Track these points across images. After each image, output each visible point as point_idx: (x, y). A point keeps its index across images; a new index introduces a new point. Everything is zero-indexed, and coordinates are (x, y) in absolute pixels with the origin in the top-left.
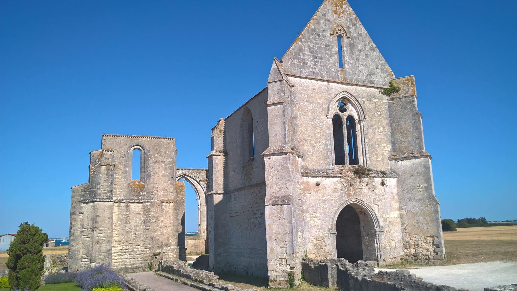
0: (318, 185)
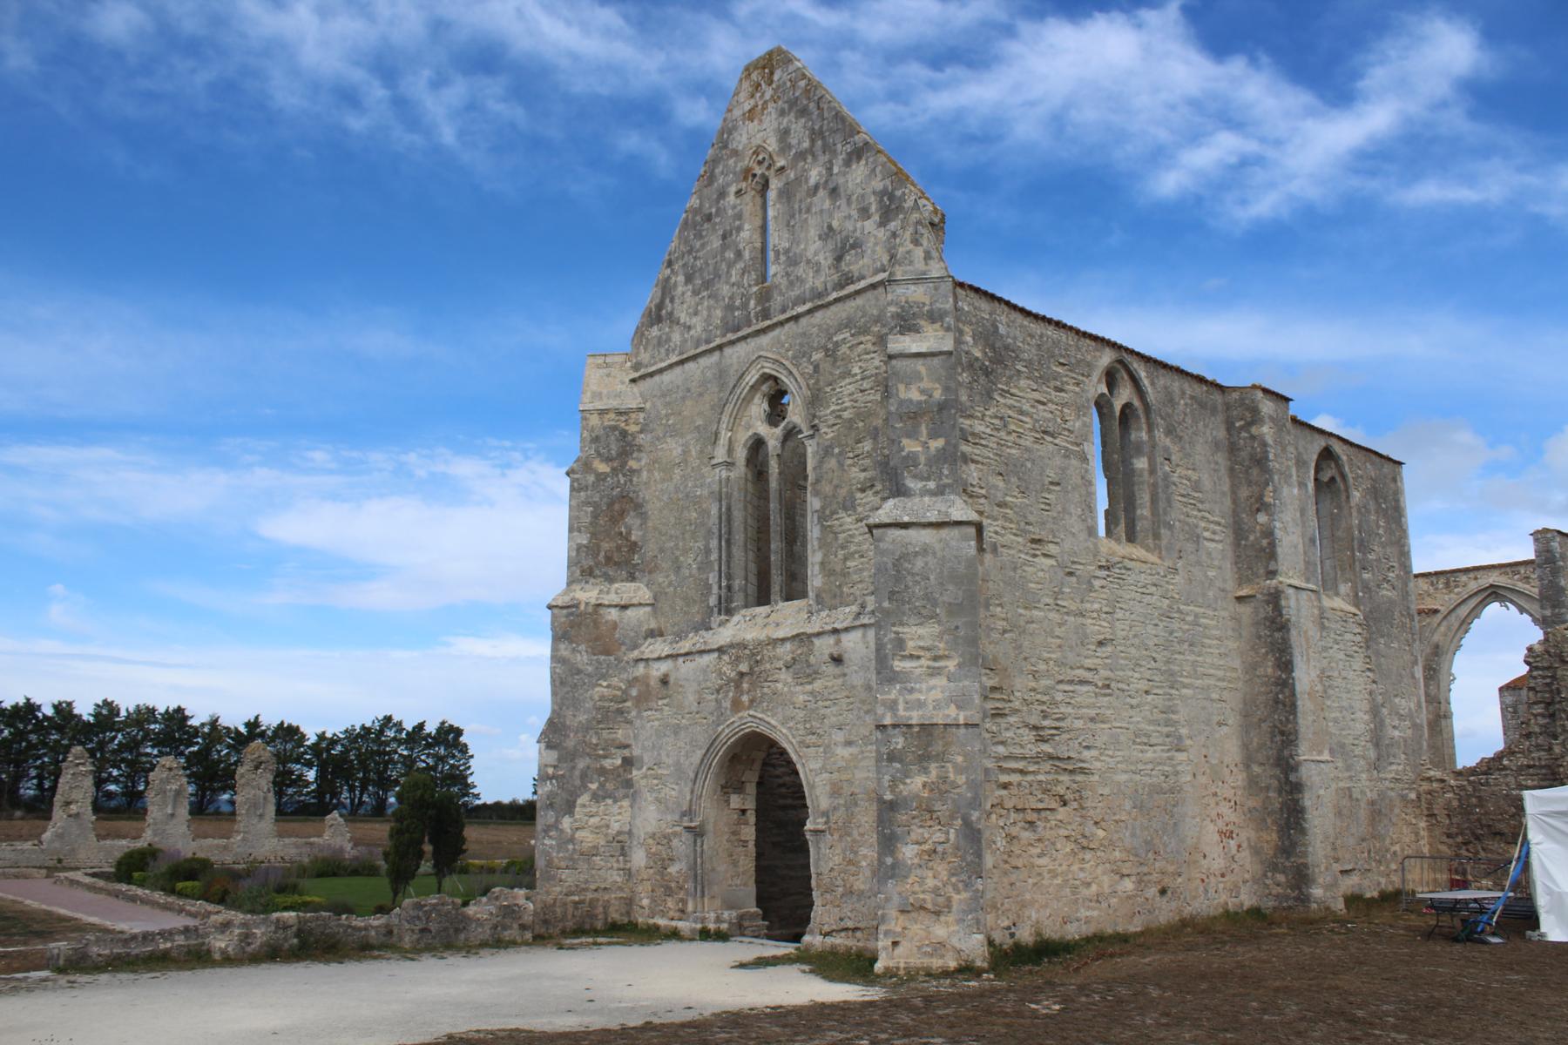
0: (664, 681)
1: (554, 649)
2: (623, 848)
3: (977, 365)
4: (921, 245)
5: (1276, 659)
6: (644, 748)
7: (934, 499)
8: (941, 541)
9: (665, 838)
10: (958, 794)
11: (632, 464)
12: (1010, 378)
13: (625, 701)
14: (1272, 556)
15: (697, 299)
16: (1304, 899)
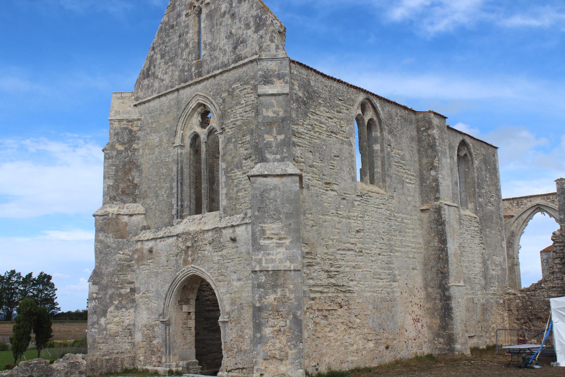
0: (151, 251)
1: (96, 236)
2: (130, 332)
3: (300, 100)
4: (274, 42)
5: (439, 239)
6: (141, 284)
7: (279, 163)
8: (283, 183)
9: (151, 327)
10: (291, 303)
11: (135, 146)
12: (316, 106)
13: (131, 261)
14: (438, 190)
15: (166, 66)
16: (452, 350)
